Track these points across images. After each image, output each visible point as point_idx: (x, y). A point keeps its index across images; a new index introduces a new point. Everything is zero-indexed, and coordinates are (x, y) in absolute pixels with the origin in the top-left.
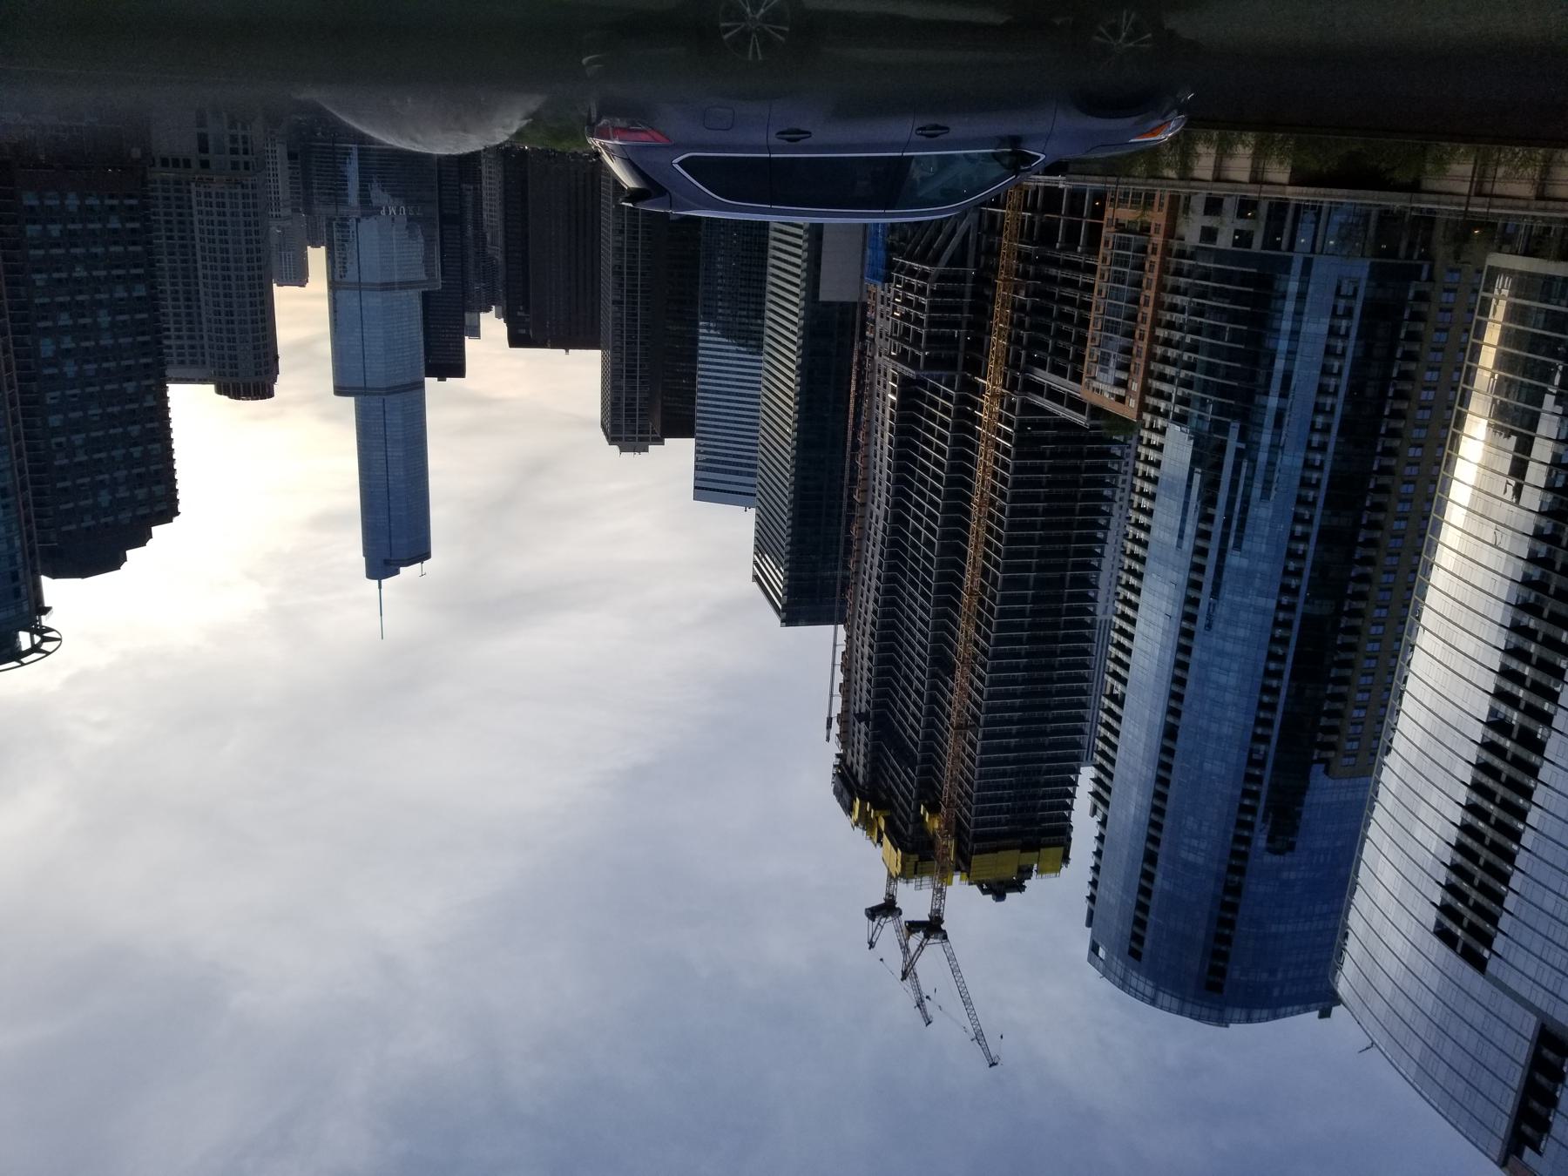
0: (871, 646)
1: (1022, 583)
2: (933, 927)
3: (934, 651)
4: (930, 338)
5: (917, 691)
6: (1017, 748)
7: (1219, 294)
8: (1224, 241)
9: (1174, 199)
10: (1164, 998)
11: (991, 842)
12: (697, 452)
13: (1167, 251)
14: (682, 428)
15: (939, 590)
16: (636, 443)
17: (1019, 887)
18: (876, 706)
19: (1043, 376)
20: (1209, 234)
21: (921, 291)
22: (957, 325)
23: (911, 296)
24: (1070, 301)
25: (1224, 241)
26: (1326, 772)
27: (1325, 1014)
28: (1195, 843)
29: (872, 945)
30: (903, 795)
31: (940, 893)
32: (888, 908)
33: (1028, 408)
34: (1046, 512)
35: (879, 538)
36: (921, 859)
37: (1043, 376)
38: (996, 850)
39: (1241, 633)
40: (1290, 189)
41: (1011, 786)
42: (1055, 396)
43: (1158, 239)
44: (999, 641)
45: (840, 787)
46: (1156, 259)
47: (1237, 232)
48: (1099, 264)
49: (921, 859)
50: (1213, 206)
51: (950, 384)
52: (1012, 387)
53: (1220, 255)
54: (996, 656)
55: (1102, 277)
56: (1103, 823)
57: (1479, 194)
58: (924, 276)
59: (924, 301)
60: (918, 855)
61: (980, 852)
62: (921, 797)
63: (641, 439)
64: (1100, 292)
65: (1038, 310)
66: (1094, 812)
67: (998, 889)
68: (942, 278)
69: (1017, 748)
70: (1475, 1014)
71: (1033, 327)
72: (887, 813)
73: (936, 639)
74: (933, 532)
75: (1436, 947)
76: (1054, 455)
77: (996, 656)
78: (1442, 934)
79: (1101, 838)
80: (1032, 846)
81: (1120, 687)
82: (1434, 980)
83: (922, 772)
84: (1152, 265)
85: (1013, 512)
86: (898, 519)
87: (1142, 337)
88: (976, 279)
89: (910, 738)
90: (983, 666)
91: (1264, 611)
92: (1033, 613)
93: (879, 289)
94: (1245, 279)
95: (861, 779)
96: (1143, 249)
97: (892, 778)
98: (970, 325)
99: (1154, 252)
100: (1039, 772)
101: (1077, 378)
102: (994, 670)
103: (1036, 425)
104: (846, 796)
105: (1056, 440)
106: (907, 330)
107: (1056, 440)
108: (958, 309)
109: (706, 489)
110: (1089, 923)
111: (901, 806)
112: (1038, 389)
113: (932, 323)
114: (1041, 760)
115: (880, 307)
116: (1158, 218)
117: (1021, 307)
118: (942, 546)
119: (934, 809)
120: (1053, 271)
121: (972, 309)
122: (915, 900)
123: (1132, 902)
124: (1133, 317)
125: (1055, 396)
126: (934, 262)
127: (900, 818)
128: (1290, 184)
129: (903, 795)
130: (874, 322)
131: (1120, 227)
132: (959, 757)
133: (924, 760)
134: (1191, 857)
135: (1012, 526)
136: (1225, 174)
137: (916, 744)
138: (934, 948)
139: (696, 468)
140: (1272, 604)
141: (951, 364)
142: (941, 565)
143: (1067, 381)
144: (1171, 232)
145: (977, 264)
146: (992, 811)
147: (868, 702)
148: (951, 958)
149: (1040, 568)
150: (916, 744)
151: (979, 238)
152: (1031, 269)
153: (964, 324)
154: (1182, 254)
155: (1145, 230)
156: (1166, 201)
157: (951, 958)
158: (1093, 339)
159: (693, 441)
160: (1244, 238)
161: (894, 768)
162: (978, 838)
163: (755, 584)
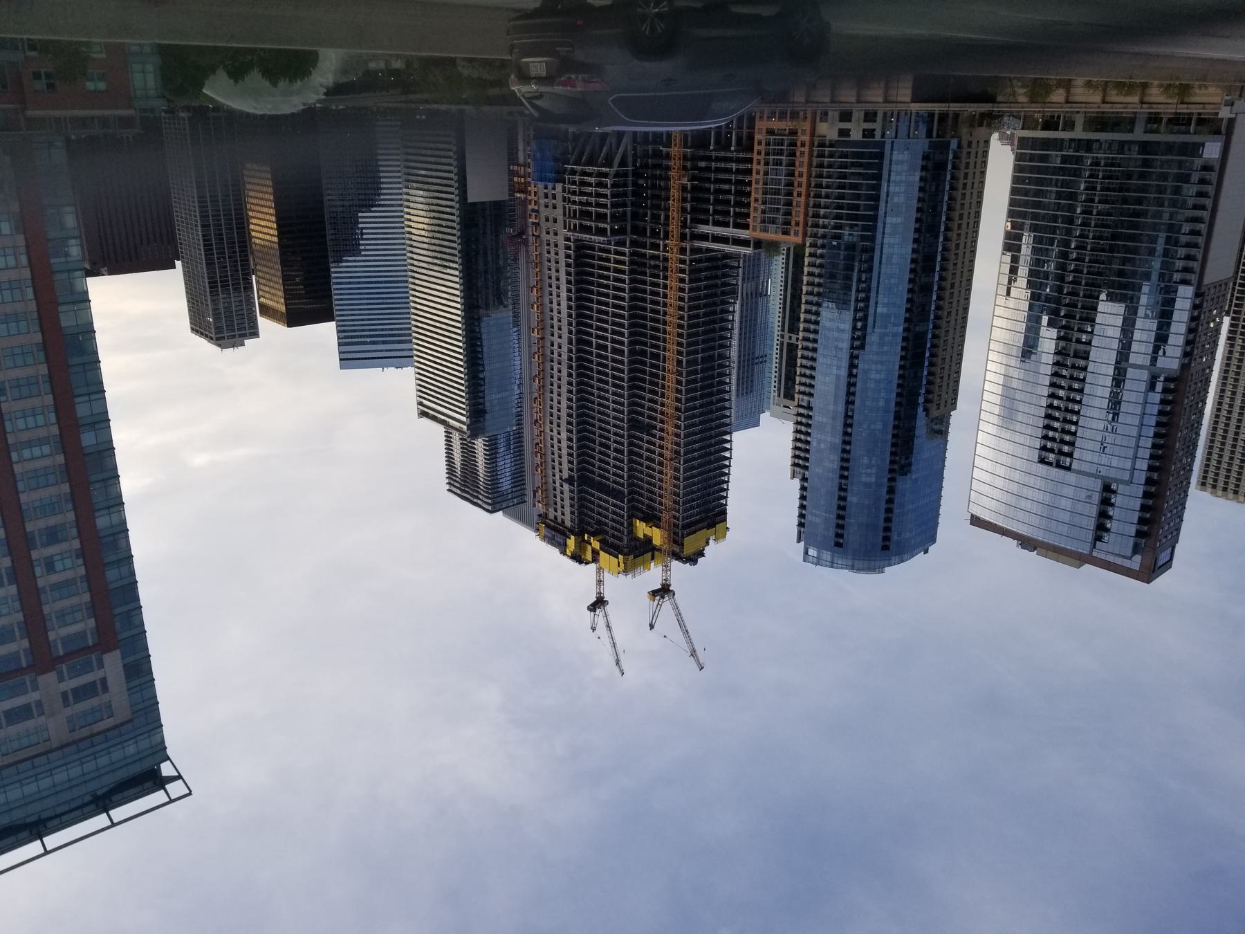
0: (569, 431)
1: (695, 362)
2: (664, 591)
3: (629, 420)
4: (613, 216)
5: (616, 450)
6: (700, 466)
7: (853, 165)
8: (856, 135)
9: (814, 114)
10: (858, 564)
11: (692, 527)
12: (338, 332)
13: (812, 144)
14: (323, 315)
15: (630, 380)
16: (238, 339)
17: (703, 555)
18: (578, 470)
19: (703, 229)
20: (844, 133)
21: (599, 185)
22: (624, 205)
23: (589, 189)
24: (729, 181)
25: (856, 135)
26: (927, 415)
27: (926, 552)
28: (869, 471)
29: (594, 629)
30: (613, 520)
31: (667, 568)
32: (599, 603)
33: (695, 251)
34: (705, 315)
35: (565, 357)
36: (635, 557)
37: (703, 229)
38: (694, 532)
39: (886, 348)
40: (913, 105)
41: (699, 490)
42: (717, 239)
43: (806, 138)
44: (687, 400)
45: (550, 533)
46: (806, 149)
47: (864, 130)
48: (755, 157)
49: (635, 557)
50: (846, 116)
51: (623, 244)
52: (683, 237)
53: (855, 144)
54: (687, 410)
55: (759, 163)
56: (804, 479)
57: (1067, 102)
58: (600, 175)
59: (608, 192)
60: (635, 553)
61: (688, 535)
62: (631, 517)
63: (241, 336)
64: (758, 173)
65: (693, 187)
66: (793, 477)
67: (692, 559)
68: (617, 175)
69: (700, 466)
70: (1069, 491)
71: (693, 199)
72: (600, 537)
73: (630, 412)
74: (622, 343)
75: (1043, 469)
76: (707, 278)
77: (687, 410)
78: (1042, 461)
79: (803, 488)
80: (712, 525)
81: (806, 398)
82: (1039, 483)
83: (629, 501)
84: (802, 153)
85: (690, 317)
86: (581, 342)
87: (799, 195)
88: (635, 174)
89: (614, 482)
90: (679, 419)
91: (895, 335)
92: (703, 379)
93: (537, 187)
94: (871, 156)
95: (568, 523)
96: (793, 144)
97: (599, 514)
98: (633, 204)
99: (803, 145)
100: (710, 478)
101: (746, 227)
102: (687, 418)
103: (699, 261)
104: (559, 538)
105: (707, 269)
106: (586, 215)
107: (707, 269)
108: (625, 194)
109: (347, 360)
110: (799, 540)
111: (613, 528)
112: (704, 237)
113: (614, 205)
114: (710, 471)
115: (543, 201)
116: (807, 126)
117: (684, 189)
118: (630, 351)
119: (652, 519)
120: (703, 164)
121: (634, 194)
122: (629, 589)
123: (833, 516)
124: (791, 184)
125: (717, 239)
126: (611, 166)
127: (613, 536)
128: (913, 101)
129: (613, 520)
130: (537, 211)
131: (770, 132)
132: (669, 482)
133: (630, 493)
134: (868, 480)
135: (690, 327)
136: (863, 99)
137: (622, 485)
138: (667, 604)
139: (339, 344)
140: (901, 329)
141: (622, 231)
142: (631, 363)
143: (731, 229)
144: (813, 134)
145: (634, 165)
146: (692, 508)
147: (571, 470)
148: (676, 607)
149: (704, 350)
150: (622, 485)
151: (635, 149)
152: (689, 164)
153: (629, 204)
154: (822, 145)
155: (793, 133)
156: (809, 116)
157: (676, 607)
158: (756, 200)
159: (333, 325)
160: (868, 133)
161: (600, 506)
162: (684, 527)
163: (425, 420)
